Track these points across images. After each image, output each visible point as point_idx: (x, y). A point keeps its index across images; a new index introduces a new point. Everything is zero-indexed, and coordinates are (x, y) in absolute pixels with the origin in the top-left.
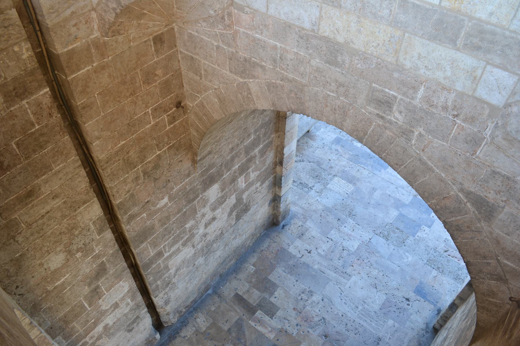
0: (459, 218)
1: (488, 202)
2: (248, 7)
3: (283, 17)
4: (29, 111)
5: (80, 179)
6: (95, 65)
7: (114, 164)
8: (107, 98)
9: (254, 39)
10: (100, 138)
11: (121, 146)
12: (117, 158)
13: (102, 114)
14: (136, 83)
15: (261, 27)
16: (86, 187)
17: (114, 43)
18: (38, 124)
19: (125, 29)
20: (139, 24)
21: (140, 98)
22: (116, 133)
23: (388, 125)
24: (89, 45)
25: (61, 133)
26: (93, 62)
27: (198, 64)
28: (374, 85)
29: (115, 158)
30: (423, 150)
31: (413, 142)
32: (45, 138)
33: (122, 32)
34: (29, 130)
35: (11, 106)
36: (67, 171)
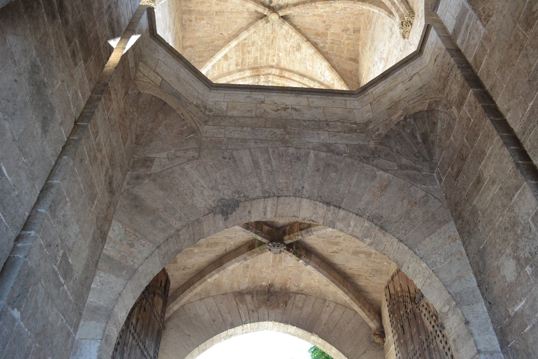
5: (506, 161)
7: (530, 133)
8: (503, 69)
10: (510, 110)
11: (531, 109)
12: (532, 125)
13: (505, 86)
14: (519, 37)
16: (513, 168)
17: (493, 26)
18: (472, 118)
19: (491, 10)
21: (529, 47)
22: (521, 97)
24: (482, 42)
29: (529, 126)
33: (491, 13)
35: (460, 112)
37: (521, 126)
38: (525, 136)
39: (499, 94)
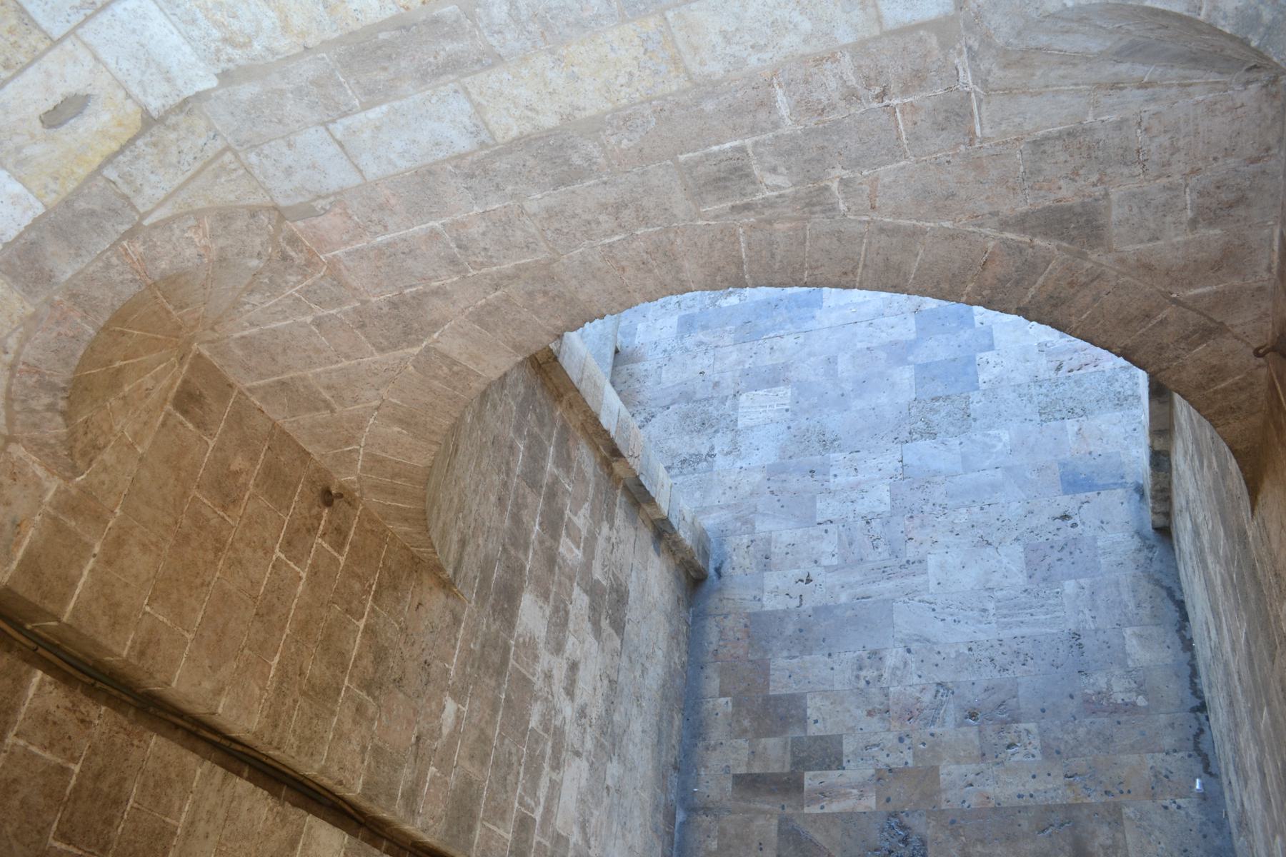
0: (1041, 280)
1: (1070, 208)
2: (319, 197)
3: (403, 164)
4: (34, 749)
5: (246, 805)
6: (97, 550)
7: (290, 717)
8: (174, 596)
9: (380, 251)
10: (223, 689)
11: (278, 670)
12: (289, 701)
13: (189, 636)
14: (208, 520)
15: (374, 217)
16: (271, 810)
17: (103, 476)
18: (74, 760)
20: (124, 397)
21: (241, 546)
22: (246, 651)
23: (768, 213)
24: (55, 519)
25: (136, 742)
26: (89, 546)
27: (305, 387)
28: (682, 158)
29: (283, 704)
30: (873, 208)
31: (842, 207)
32: (112, 778)
33: (101, 441)
34: (65, 787)
36: (207, 808)
37: (265, 713)
38: (279, 730)
39: (174, 662)
